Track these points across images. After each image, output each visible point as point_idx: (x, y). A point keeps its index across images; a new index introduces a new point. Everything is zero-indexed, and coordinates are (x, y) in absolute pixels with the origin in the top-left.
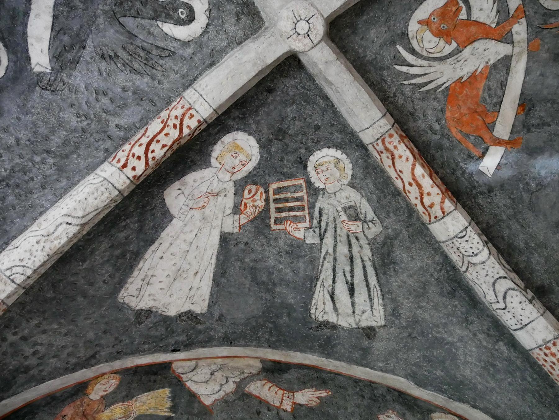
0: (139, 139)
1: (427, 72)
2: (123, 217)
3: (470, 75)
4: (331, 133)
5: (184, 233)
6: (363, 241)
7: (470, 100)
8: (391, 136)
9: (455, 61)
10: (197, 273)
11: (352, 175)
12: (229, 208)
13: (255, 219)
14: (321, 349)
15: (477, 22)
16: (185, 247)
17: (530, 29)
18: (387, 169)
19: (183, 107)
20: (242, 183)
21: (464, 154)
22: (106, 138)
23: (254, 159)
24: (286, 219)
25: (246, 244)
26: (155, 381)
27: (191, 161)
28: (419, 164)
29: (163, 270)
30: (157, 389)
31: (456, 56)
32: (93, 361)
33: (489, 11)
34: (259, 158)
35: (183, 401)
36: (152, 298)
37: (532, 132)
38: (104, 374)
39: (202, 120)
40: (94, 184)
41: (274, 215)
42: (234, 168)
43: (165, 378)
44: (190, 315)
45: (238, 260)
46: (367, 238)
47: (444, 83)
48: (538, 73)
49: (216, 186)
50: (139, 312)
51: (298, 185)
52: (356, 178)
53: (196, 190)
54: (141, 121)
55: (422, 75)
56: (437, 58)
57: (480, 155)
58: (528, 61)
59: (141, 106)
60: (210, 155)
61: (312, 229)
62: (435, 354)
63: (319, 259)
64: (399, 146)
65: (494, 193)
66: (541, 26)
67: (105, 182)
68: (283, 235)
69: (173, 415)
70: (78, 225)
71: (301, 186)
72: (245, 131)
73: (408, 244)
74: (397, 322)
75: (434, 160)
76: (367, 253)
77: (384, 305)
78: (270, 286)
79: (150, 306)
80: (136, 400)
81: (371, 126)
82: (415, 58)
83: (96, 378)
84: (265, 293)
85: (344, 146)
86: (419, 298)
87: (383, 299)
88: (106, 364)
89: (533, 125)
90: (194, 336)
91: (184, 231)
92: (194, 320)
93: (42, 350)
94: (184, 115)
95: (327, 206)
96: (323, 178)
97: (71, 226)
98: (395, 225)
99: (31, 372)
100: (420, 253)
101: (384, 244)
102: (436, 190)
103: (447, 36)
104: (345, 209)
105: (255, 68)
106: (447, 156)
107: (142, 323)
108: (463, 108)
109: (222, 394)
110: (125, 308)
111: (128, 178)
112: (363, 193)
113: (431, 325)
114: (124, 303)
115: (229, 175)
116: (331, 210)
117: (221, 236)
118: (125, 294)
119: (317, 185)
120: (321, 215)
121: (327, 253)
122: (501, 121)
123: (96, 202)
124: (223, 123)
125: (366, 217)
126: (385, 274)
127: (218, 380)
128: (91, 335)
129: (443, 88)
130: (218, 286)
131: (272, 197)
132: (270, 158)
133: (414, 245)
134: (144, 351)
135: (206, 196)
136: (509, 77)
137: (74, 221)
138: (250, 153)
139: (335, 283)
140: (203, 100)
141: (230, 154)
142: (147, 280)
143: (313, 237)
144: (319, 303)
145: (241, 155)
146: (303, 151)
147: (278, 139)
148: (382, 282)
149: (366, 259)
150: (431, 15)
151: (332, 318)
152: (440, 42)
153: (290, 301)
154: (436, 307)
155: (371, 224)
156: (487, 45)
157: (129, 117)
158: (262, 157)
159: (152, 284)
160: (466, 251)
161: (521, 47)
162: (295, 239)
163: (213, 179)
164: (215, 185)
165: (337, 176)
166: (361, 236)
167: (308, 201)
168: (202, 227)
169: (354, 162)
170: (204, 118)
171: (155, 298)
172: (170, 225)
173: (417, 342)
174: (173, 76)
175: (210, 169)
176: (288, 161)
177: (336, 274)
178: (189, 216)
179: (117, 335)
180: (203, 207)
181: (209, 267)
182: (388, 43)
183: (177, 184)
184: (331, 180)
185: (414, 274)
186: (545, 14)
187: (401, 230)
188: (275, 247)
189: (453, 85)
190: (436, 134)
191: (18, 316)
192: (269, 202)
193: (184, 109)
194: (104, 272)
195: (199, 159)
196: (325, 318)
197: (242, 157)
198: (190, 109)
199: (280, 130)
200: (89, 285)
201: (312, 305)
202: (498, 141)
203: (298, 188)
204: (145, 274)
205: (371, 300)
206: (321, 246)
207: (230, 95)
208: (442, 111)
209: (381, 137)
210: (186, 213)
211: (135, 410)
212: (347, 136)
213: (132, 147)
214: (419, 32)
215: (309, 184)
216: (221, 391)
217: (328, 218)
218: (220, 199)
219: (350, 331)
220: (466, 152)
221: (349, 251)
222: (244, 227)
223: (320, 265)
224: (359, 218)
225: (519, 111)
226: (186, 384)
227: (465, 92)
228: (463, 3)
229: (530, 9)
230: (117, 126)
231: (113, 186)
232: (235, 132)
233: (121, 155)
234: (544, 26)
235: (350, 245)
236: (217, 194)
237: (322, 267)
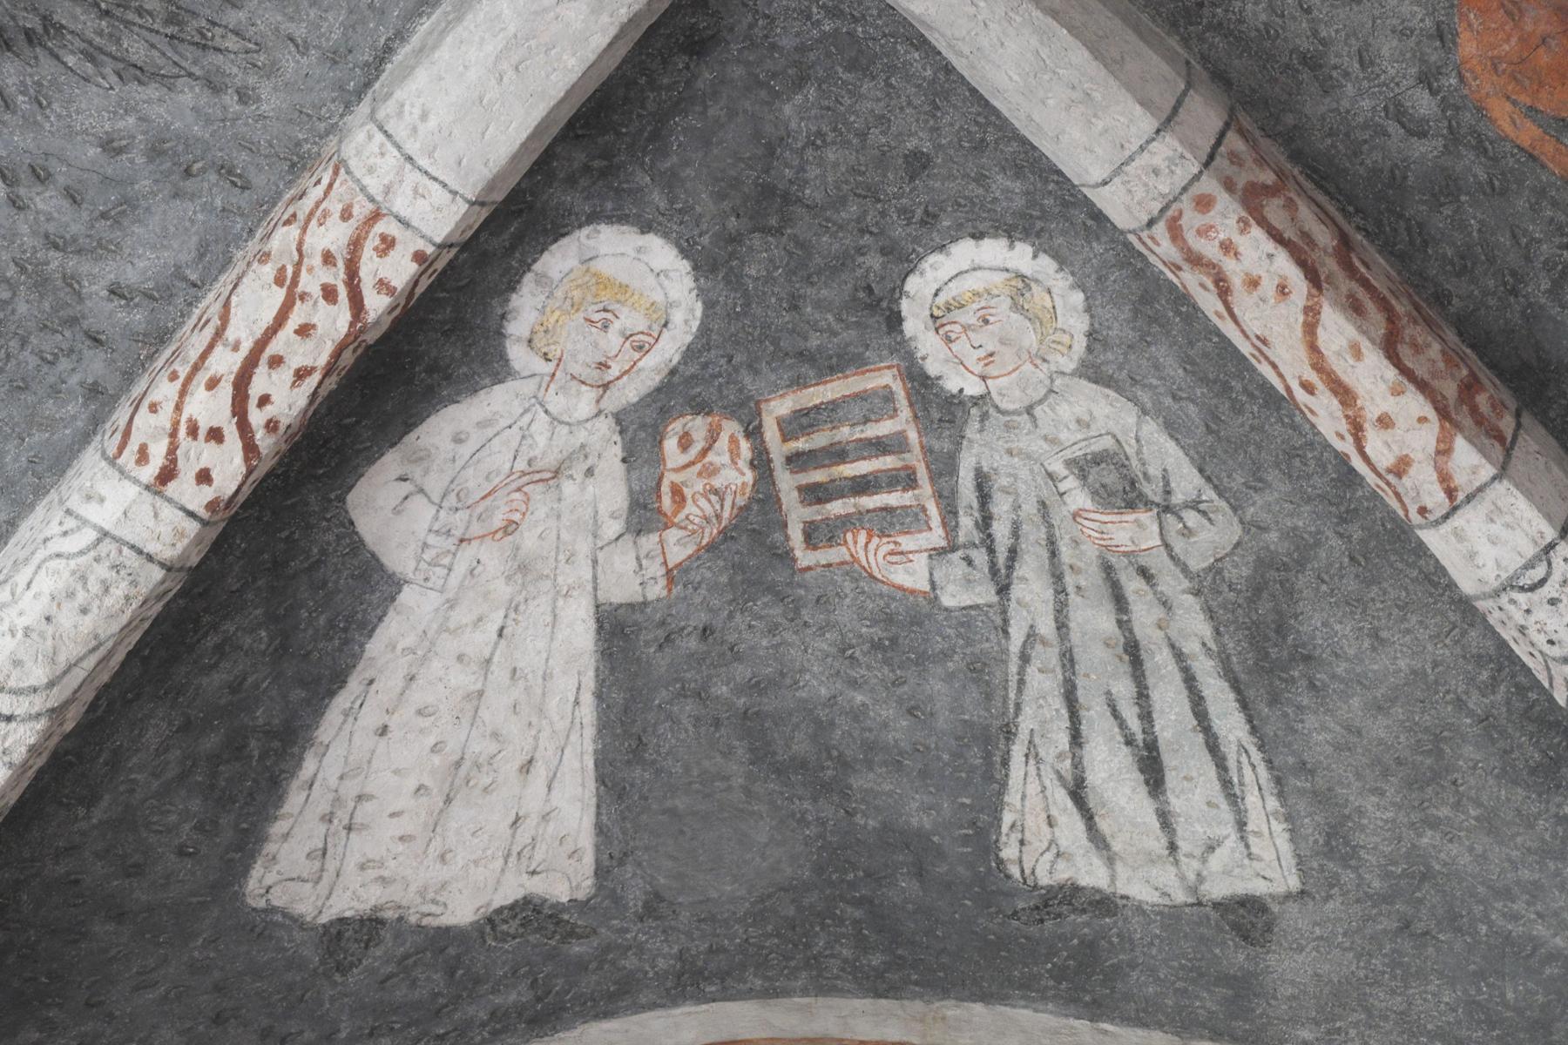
0: (204, 356)
2: (206, 619)
4: (981, 179)
5: (454, 632)
6: (1172, 583)
8: (1204, 203)
10: (530, 762)
11: (1089, 335)
12: (613, 516)
13: (725, 540)
14: (1064, 985)
16: (464, 679)
19: (346, 215)
20: (650, 415)
22: (84, 346)
23: (678, 317)
24: (846, 522)
25: (706, 632)
27: (431, 370)
28: (1335, 303)
29: (396, 772)
34: (699, 313)
36: (372, 874)
39: (430, 250)
40: (69, 557)
41: (797, 515)
42: (603, 366)
44: (528, 911)
45: (682, 694)
46: (1185, 569)
49: (545, 444)
50: (333, 931)
51: (874, 392)
52: (1106, 345)
53: (470, 471)
54: (201, 256)
59: (192, 197)
60: (500, 335)
61: (960, 553)
62: (1510, 995)
63: (1005, 662)
64: (1242, 242)
67: (107, 547)
68: (848, 586)
70: (38, 716)
71: (888, 397)
72: (618, 218)
73: (1351, 585)
74: (1348, 877)
75: (1425, 243)
76: (1194, 626)
77: (1288, 818)
78: (830, 773)
79: (373, 902)
81: (1118, 171)
84: (815, 800)
85: (1039, 224)
86: (1421, 789)
87: (1281, 795)
90: (560, 981)
91: (452, 626)
92: (551, 927)
94: (356, 245)
95: (1006, 459)
96: (972, 358)
97: (13, 725)
98: (1291, 515)
100: (1404, 619)
101: (1257, 589)
102: (1414, 404)
104: (1082, 467)
105: (605, 19)
107: (352, 965)
110: (276, 924)
111: (191, 514)
112: (1145, 397)
113: (1480, 889)
114: (271, 910)
115: (589, 395)
116: (1024, 473)
117: (598, 620)
118: (270, 879)
119: (952, 384)
120: (984, 497)
121: (1032, 636)
123: (87, 623)
124: (531, 207)
125: (1168, 492)
126: (1274, 700)
130: (620, 797)
131: (777, 449)
132: (747, 305)
133: (1375, 589)
135: (514, 486)
137: (22, 706)
138: (658, 297)
139: (1080, 745)
140: (418, 176)
141: (581, 315)
142: (342, 816)
143: (968, 582)
144: (1030, 822)
145: (624, 312)
146: (874, 261)
147: (766, 230)
148: (1269, 730)
149: (1191, 647)
151: (1091, 874)
153: (914, 821)
154: (1489, 823)
155: (1191, 518)
157: (154, 247)
158: (709, 305)
159: (364, 827)
160: (1551, 642)
162: (899, 594)
163: (527, 418)
164: (542, 441)
165: (1026, 343)
166: (1159, 562)
167: (927, 451)
168: (521, 598)
169: (1090, 283)
170: (438, 240)
171: (386, 873)
172: (391, 613)
173: (1438, 950)
174: (290, 63)
175: (511, 385)
176: (818, 305)
177: (1083, 713)
178: (461, 568)
180: (510, 528)
181: (574, 738)
183: (391, 463)
184: (1007, 357)
185: (1393, 701)
187: (1319, 532)
188: (822, 630)
190: (1422, 135)
192: (771, 471)
193: (353, 223)
194: (173, 818)
195: (458, 354)
196: (1063, 873)
197: (630, 319)
198: (376, 216)
199: (767, 191)
200: (129, 876)
201: (1005, 828)
203: (879, 404)
204: (331, 796)
205: (1234, 798)
206: (1004, 612)
207: (524, 136)
208: (1441, 37)
209: (1162, 211)
210: (446, 561)
212: (1046, 181)
213: (183, 393)
215: (921, 383)
217: (1017, 507)
218: (569, 488)
219: (1171, 916)
221: (1120, 623)
222: (687, 571)
223: (1013, 685)
224: (1141, 495)
230: (115, 291)
231: (140, 552)
232: (586, 231)
233: (150, 428)
235: (1120, 602)
236: (557, 473)
237: (1020, 691)
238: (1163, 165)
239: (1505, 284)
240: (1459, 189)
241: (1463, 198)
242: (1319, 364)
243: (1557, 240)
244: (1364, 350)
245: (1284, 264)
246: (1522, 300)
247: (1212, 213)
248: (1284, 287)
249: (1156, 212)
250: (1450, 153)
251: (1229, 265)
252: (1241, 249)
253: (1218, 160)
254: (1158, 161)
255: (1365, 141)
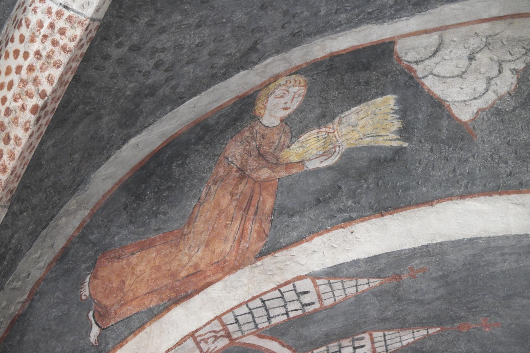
26: (367, 83)
30: (374, 98)
32: (254, 56)
35: (420, 116)
38: (277, 77)
43: (385, 75)
69: (406, 145)
80: (340, 123)
83: (266, 85)
88: (277, 57)
93: (167, 57)
99: (161, 92)
109: (491, 97)
127: (483, 70)
128: (240, 17)
134: (340, 24)
179: (285, 8)
191: (116, 20)
211: (340, 140)
216: (490, 92)
226: (423, 84)
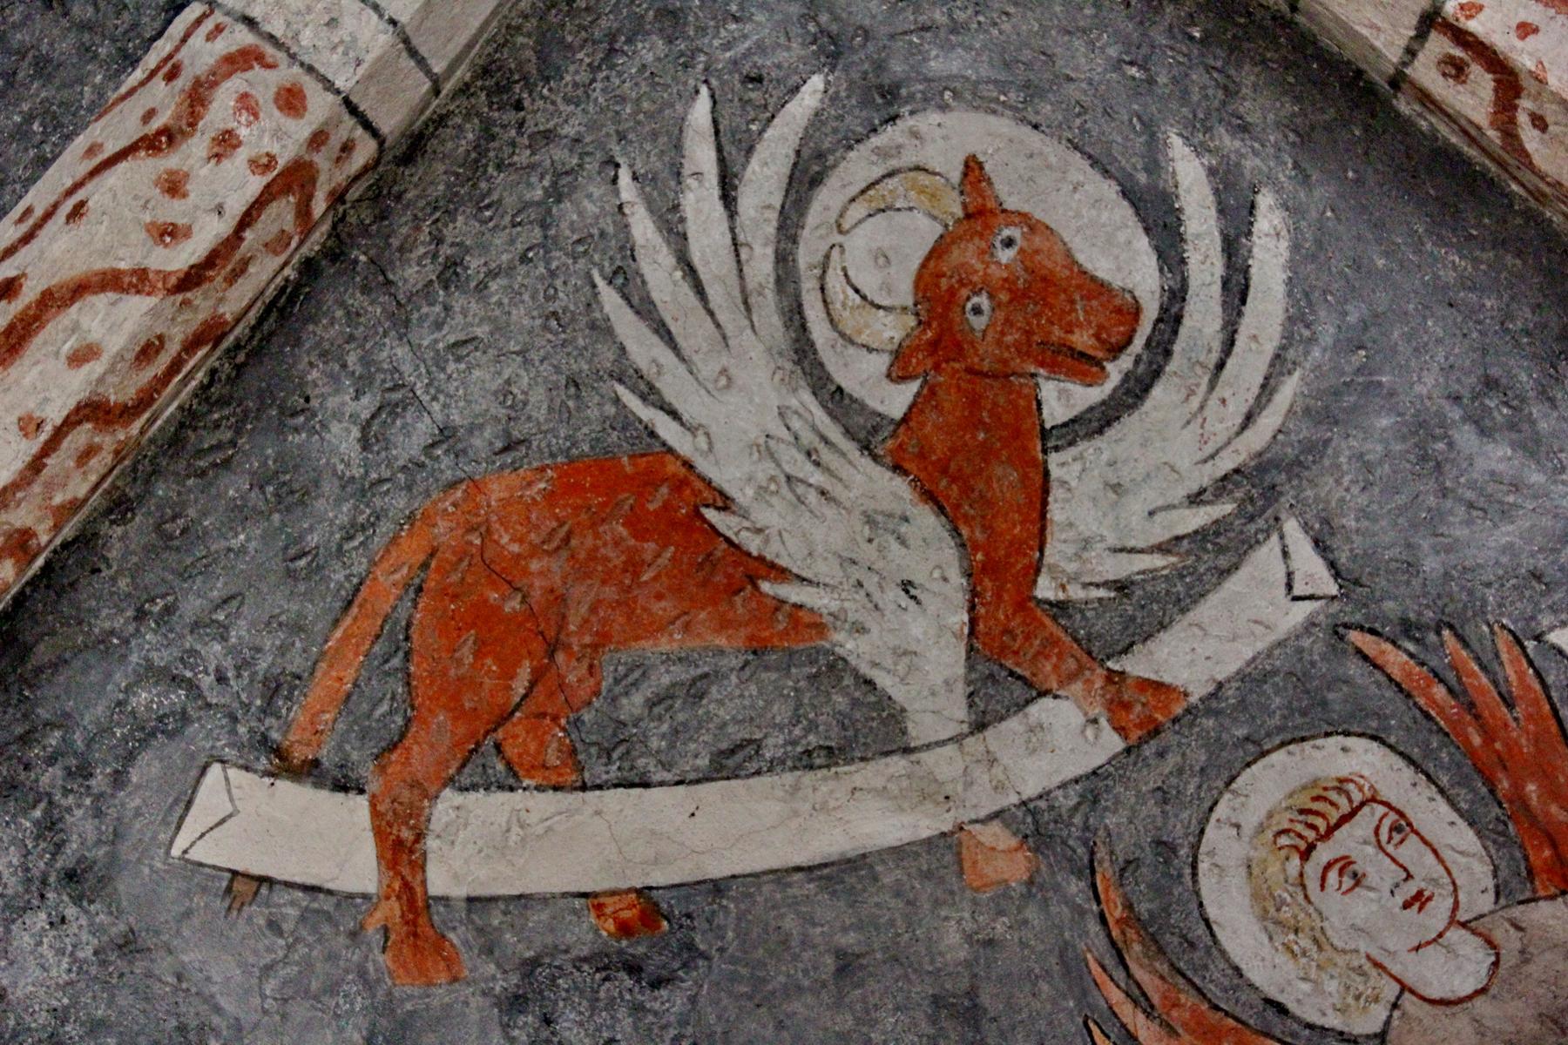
1: (714, 293)
3: (753, 545)
7: (610, 592)
9: (808, 438)
15: (1046, 491)
17: (1066, 801)
18: (81, 142)
21: (283, 650)
31: (835, 433)
33: (1112, 540)
37: (505, 1027)
47: (674, 414)
48: (850, 940)
55: (690, 271)
56: (804, 327)
57: (299, 754)
58: (899, 852)
65: (71, 911)
66: (1101, 853)
75: (202, 474)
82: (777, 201)
89: (547, 1021)
103: (934, 345)
106: (243, 550)
108: (557, 565)
122: (533, 818)
129: (646, 413)
136: (789, 778)
150: (1024, 218)
152: (890, 319)
156: (937, 586)
161: (969, 785)
182: (824, 18)
186: (1165, 848)
189: (673, 467)
190: (365, 443)
202: (407, 834)
208: (506, 449)
209: (271, 38)
214: (923, 178)
220: (296, 663)
225: (611, 905)
227: (650, 547)
228: (1127, 377)
229: (1172, 760)
234: (1105, 871)
238: (342, 33)
239: (152, 601)
240: (288, 509)
241: (276, 517)
242: (53, 301)
243: (228, 663)
244: (86, 368)
245: (208, 233)
246: (131, 628)
247: (277, 113)
248: (171, 234)
249: (267, 28)
250: (343, 488)
251: (196, 147)
252: (226, 163)
253: (349, 121)
254: (348, 24)
255: (344, 366)
